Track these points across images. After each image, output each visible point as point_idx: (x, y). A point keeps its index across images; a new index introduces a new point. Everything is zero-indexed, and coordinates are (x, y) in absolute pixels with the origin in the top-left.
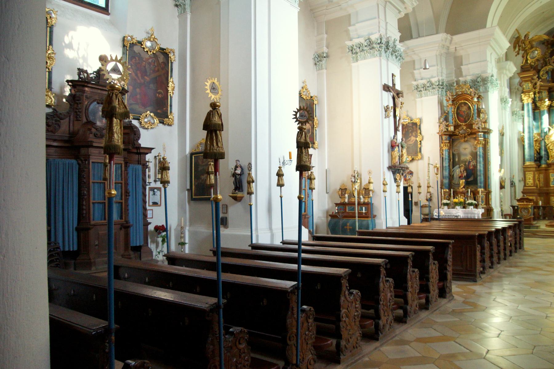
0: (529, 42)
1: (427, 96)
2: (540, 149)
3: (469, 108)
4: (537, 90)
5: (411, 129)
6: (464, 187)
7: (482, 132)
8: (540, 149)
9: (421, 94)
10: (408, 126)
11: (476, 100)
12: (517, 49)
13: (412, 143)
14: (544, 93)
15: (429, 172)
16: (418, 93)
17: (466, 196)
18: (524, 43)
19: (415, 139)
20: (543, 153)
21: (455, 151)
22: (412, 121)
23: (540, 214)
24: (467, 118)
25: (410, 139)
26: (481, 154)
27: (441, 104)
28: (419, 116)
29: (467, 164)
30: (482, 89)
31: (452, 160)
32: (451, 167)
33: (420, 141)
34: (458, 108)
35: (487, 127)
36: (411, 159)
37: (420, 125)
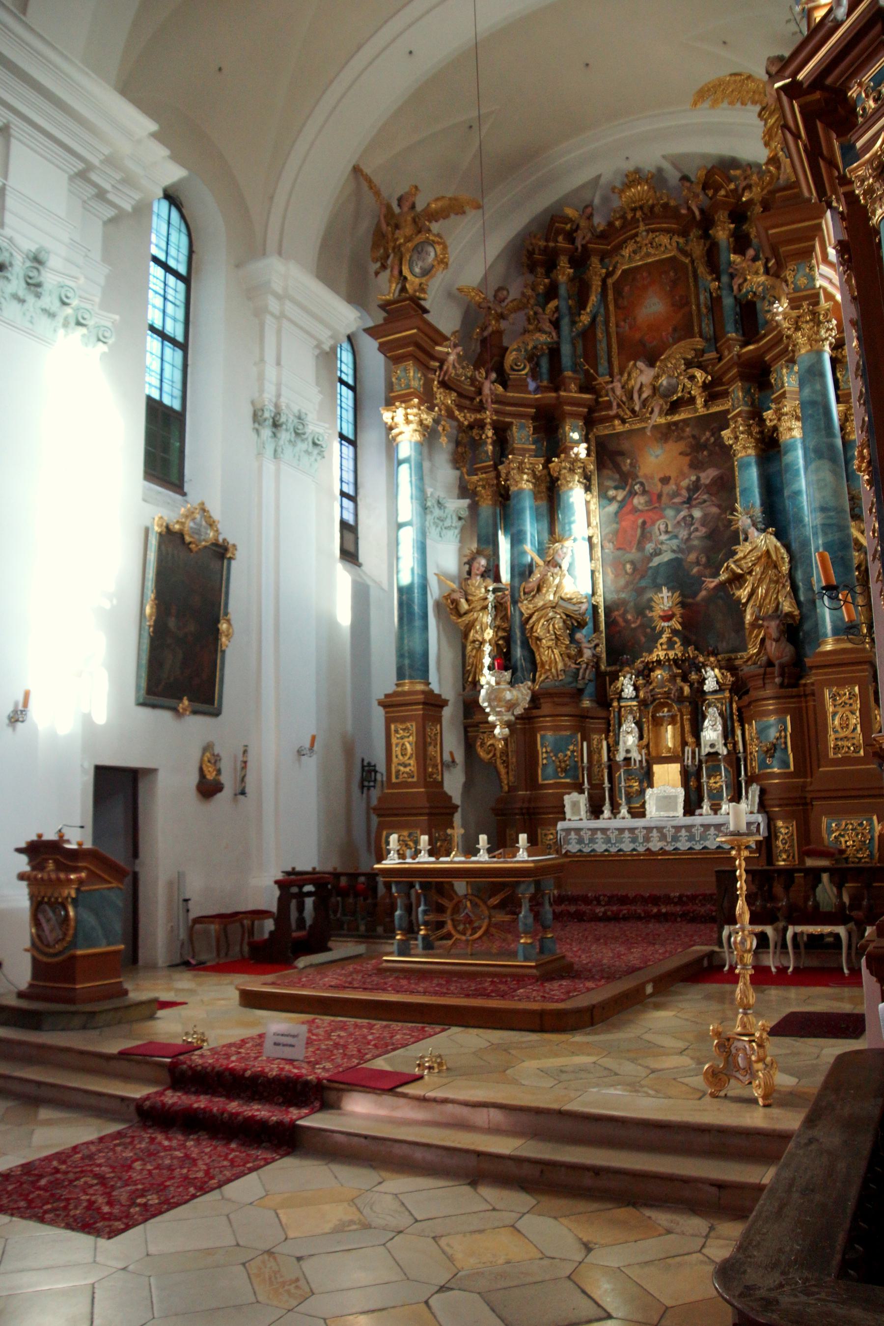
14: (522, 427)
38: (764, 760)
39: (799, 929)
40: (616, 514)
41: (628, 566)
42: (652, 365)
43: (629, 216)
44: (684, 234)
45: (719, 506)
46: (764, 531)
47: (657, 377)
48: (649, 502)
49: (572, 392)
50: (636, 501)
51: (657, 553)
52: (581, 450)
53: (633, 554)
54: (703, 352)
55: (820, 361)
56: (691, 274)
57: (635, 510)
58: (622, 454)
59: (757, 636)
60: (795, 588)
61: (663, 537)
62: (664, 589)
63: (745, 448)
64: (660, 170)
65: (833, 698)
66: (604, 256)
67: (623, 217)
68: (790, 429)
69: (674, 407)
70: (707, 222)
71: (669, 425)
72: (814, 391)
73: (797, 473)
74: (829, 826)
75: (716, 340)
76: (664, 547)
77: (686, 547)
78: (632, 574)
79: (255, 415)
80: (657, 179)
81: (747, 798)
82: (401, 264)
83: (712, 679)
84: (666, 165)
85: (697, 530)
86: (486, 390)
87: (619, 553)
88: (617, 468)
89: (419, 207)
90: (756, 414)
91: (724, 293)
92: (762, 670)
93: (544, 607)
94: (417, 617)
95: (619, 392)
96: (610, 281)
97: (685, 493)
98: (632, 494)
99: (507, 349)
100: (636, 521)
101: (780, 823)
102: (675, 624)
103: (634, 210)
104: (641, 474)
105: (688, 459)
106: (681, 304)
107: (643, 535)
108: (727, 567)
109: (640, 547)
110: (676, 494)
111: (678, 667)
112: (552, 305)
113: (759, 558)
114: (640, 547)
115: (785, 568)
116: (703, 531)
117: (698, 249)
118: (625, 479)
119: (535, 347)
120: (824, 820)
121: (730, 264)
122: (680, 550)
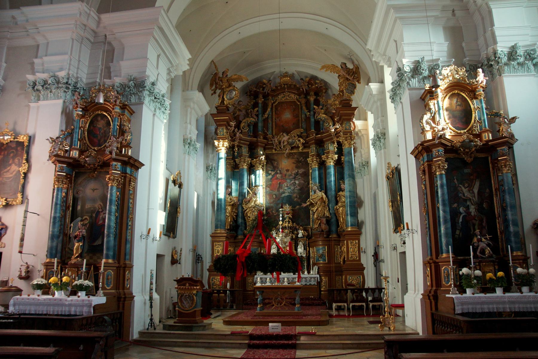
0: (227, 80)
1: (47, 100)
2: (237, 216)
3: (108, 124)
4: (236, 143)
5: (13, 152)
6: (80, 256)
7: (116, 160)
8: (237, 216)
9: (39, 97)
10: (11, 146)
11: (118, 109)
12: (214, 87)
13: (11, 176)
15: (24, 225)
16: (34, 94)
17: (80, 273)
18: (221, 81)
19: (17, 169)
20: (240, 221)
21: (77, 193)
22: (17, 138)
23: (227, 301)
24: (102, 140)
25: (9, 168)
26: (114, 198)
27: (67, 114)
28: (30, 132)
29: (94, 215)
30: (133, 99)
31: (71, 209)
32: (68, 220)
33: (25, 174)
34: (92, 123)
35: (130, 154)
36: (4, 204)
37: (29, 146)
38: (318, 259)
39: (353, 304)
40: (271, 179)
41: (274, 196)
42: (287, 135)
43: (283, 86)
44: (299, 95)
45: (304, 181)
46: (321, 191)
47: (289, 139)
48: (281, 177)
49: (261, 139)
50: (278, 176)
51: (284, 193)
52: (263, 158)
53: (276, 192)
54: (302, 133)
55: (351, 150)
56: (300, 108)
57: (277, 178)
58: (274, 160)
59: (318, 222)
60: (329, 209)
61: (286, 188)
62: (287, 205)
63: (315, 165)
64: (293, 74)
65: (351, 243)
66: (273, 96)
67: (281, 86)
68: (330, 162)
69: (292, 148)
70: (307, 94)
71: (290, 153)
72: (349, 158)
73: (331, 176)
74: (349, 278)
75: (307, 130)
76: (286, 191)
77: (293, 192)
78: (275, 198)
79: (184, 140)
80: (292, 76)
81: (313, 270)
82: (224, 95)
83: (301, 233)
84: (295, 73)
85: (297, 187)
86: (237, 136)
87: (271, 191)
88: (272, 164)
89: (229, 76)
90: (319, 155)
91: (312, 117)
92: (320, 233)
93: (251, 207)
94: (223, 209)
95: (276, 141)
96: (274, 105)
97: (293, 175)
98: (277, 173)
99: (241, 121)
100: (277, 182)
101: (323, 278)
102: (290, 215)
103: (284, 84)
104: (280, 167)
105: (295, 165)
106: (297, 116)
107: (279, 187)
108: (309, 201)
109: (278, 191)
110: (291, 175)
111: (291, 229)
112: (256, 109)
113: (319, 199)
114: (278, 191)
115: (327, 203)
116: (299, 188)
117: (303, 101)
118: (275, 168)
119: (250, 123)
120: (348, 276)
121: (314, 108)
122: (291, 193)
